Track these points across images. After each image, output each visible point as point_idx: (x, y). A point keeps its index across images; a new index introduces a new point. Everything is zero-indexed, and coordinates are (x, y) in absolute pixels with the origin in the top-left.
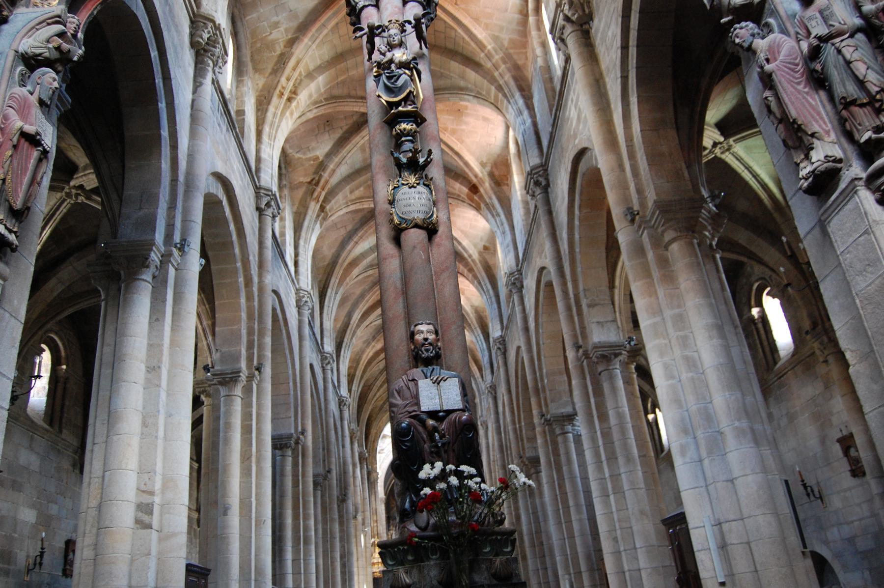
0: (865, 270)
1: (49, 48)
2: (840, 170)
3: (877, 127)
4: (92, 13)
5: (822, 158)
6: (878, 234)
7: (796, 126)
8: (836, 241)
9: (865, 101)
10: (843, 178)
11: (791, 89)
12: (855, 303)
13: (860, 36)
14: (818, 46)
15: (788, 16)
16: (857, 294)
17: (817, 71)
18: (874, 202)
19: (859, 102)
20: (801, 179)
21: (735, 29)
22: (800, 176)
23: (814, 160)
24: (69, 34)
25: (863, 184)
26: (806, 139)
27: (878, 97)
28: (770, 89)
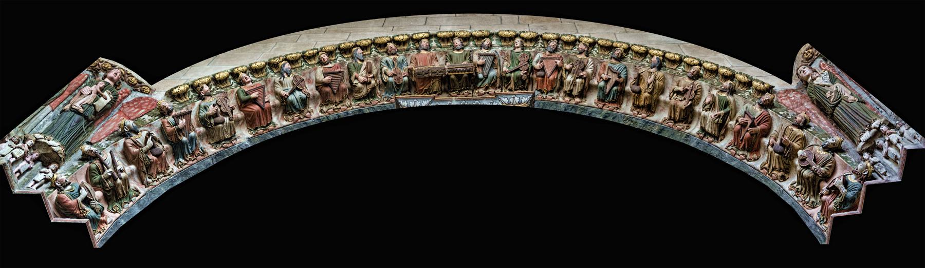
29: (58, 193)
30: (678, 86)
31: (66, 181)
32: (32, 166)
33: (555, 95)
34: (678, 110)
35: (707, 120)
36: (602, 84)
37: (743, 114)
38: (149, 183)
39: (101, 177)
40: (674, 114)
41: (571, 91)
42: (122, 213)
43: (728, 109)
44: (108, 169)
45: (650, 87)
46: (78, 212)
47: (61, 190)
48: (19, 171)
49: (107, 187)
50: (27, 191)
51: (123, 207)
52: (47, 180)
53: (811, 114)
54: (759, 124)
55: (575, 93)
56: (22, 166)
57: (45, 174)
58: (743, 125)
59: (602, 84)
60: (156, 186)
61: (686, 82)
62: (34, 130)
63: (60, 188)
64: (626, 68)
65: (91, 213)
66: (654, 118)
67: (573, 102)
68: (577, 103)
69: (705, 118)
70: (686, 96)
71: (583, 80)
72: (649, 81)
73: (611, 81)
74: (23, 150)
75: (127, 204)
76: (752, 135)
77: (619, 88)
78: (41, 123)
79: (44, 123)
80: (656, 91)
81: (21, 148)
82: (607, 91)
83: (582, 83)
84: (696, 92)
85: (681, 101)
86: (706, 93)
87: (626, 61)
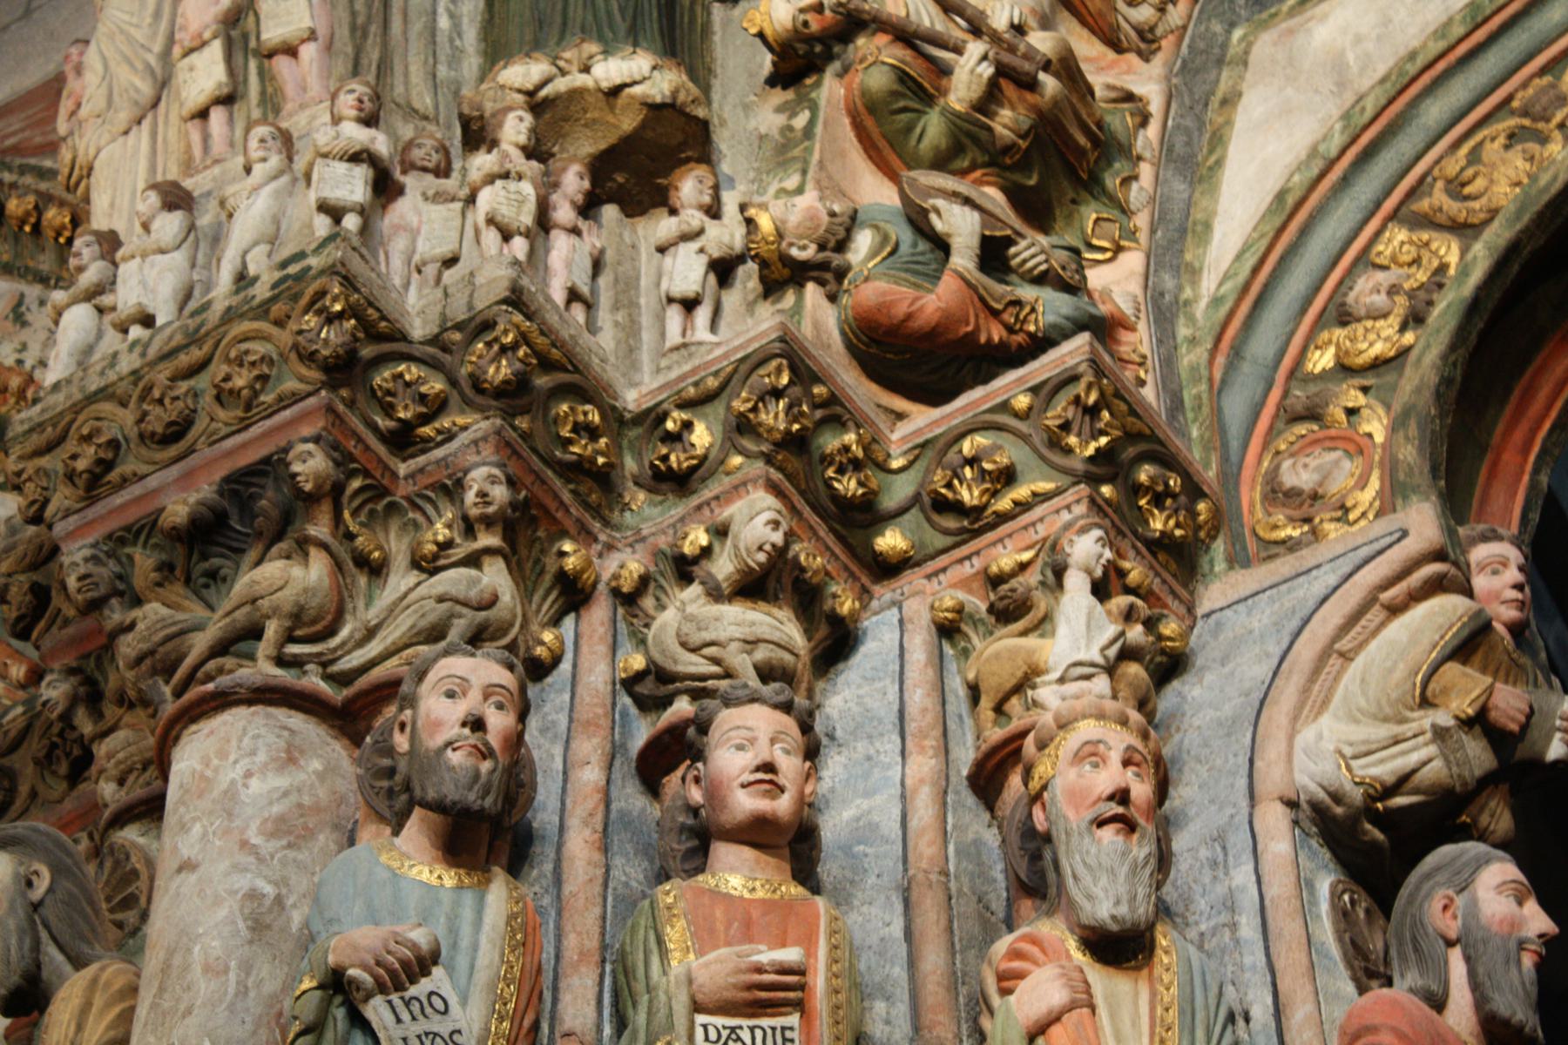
1: (1440, 734)
4: (1533, 486)
24: (1499, 627)
29: (832, 298)
31: (832, 214)
32: (598, 245)
38: (1152, 29)
39: (953, 117)
42: (1143, 236)
44: (958, 50)
46: (997, 333)
47: (841, 274)
48: (573, 295)
49: (1009, 149)
50: (687, 368)
51: (1126, 211)
52: (723, 270)
56: (569, 264)
57: (694, 246)
60: (1185, 28)
62: (443, 71)
63: (824, 266)
65: (1050, 306)
74: (520, 177)
75: (1135, 186)
78: (444, 22)
79: (452, 16)
81: (506, 176)
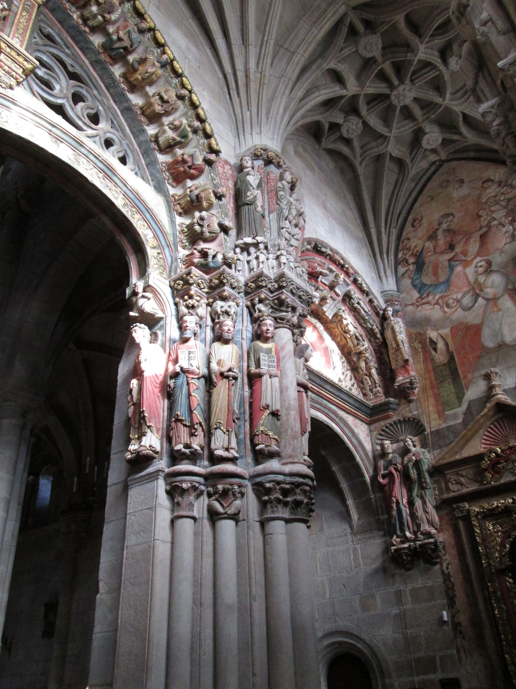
0: (139, 533)
2: (154, 458)
3: (187, 444)
5: (148, 446)
6: (158, 513)
7: (142, 415)
8: (130, 503)
9: (188, 424)
10: (153, 464)
11: (151, 388)
12: (123, 552)
13: (203, 380)
14: (179, 372)
15: (170, 340)
16: (127, 547)
17: (170, 387)
18: (164, 491)
19: (184, 423)
20: (128, 451)
21: (136, 326)
22: (129, 449)
23: (142, 444)
25: (163, 476)
26: (144, 427)
27: (196, 426)
28: (138, 379)
30: (165, 92)
33: (73, 9)
34: (152, 108)
35: (164, 134)
36: (115, 37)
37: (191, 154)
40: (147, 109)
41: (88, 19)
43: (183, 140)
45: (147, 75)
53: (228, 192)
54: (194, 169)
55: (91, 23)
58: (184, 161)
59: (115, 37)
61: (171, 95)
64: (140, 42)
66: (131, 96)
67: (83, 28)
68: (85, 32)
69: (164, 132)
70: (165, 105)
71: (103, 21)
72: (149, 70)
73: (123, 42)
76: (184, 171)
77: (124, 53)
80: (148, 81)
82: (115, 46)
83: (100, 22)
84: (173, 108)
85: (159, 105)
86: (177, 115)
87: (144, 37)
